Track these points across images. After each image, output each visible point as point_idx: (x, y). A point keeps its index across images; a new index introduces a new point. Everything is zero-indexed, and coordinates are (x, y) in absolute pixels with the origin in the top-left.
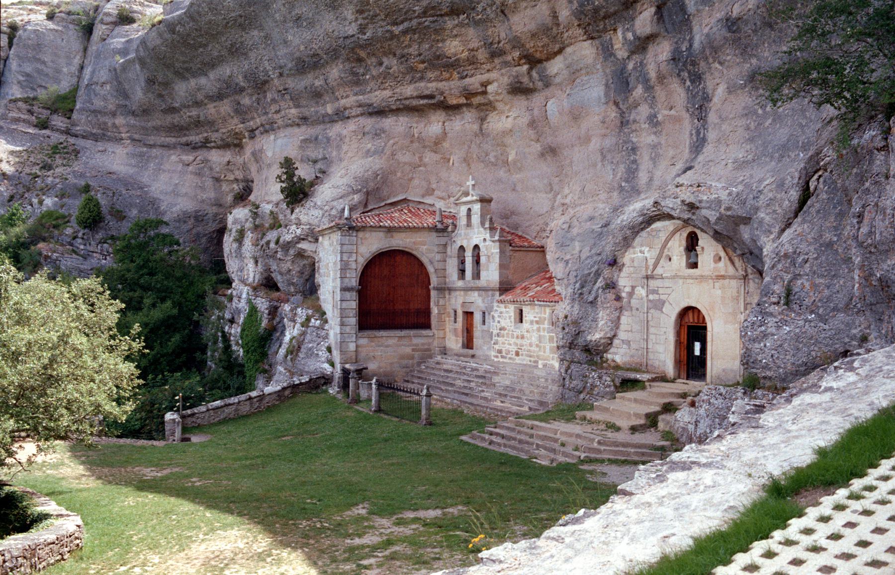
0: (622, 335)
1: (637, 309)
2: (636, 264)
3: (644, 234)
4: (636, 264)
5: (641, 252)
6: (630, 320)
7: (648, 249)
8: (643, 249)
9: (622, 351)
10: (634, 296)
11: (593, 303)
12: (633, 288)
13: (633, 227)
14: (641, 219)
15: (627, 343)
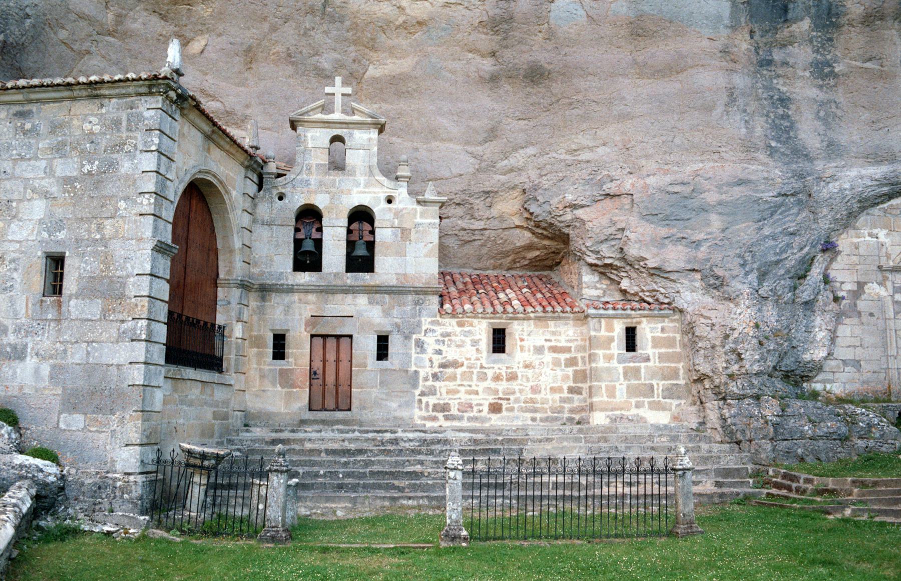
0: (842, 353)
1: (871, 315)
2: (862, 251)
3: (876, 211)
4: (862, 251)
5: (870, 235)
6: (858, 331)
7: (885, 231)
8: (875, 231)
9: (842, 377)
10: (863, 297)
11: (808, 305)
12: (861, 285)
13: (866, 199)
14: (885, 189)
15: (857, 364)
